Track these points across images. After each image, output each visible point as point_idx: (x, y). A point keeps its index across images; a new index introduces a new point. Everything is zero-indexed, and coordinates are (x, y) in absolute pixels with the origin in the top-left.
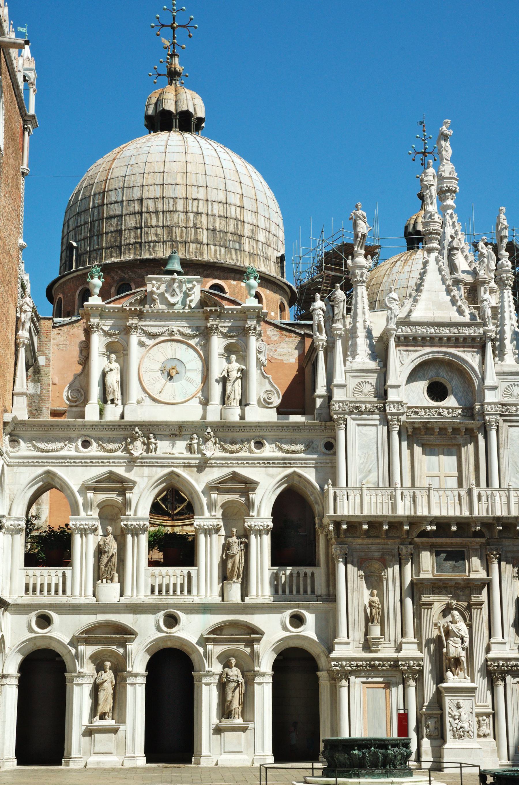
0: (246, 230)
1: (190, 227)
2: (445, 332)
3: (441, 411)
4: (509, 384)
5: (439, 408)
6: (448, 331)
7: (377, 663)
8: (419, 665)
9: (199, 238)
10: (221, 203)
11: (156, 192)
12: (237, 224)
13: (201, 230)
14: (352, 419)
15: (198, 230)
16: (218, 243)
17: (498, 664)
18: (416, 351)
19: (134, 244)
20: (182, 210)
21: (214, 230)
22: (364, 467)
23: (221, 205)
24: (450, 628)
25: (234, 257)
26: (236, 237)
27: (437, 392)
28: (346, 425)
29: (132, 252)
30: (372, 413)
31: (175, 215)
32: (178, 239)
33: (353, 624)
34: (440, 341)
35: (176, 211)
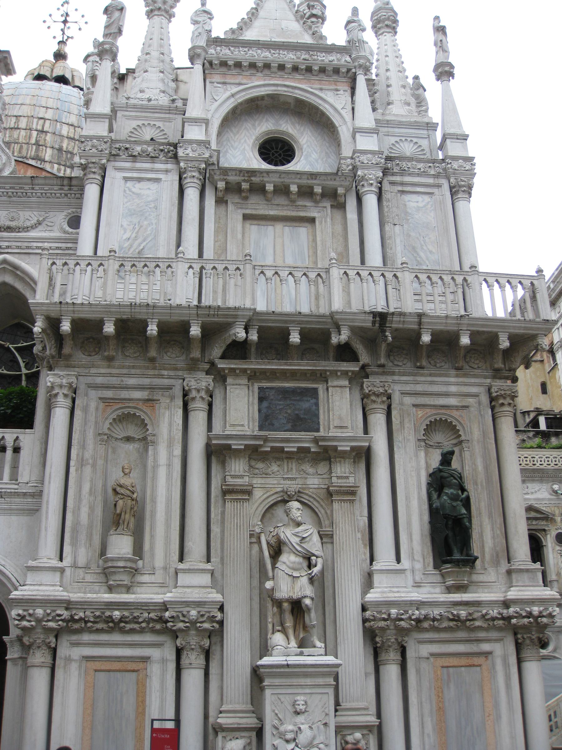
1: (31, 144)
2: (289, 57)
4: (398, 139)
7: (117, 614)
8: (212, 619)
9: (40, 154)
10: (72, 125)
13: (44, 148)
14: (116, 169)
15: (41, 147)
17: (389, 615)
18: (240, 84)
20: (24, 128)
21: (60, 150)
22: (131, 246)
24: (282, 536)
27: (277, 150)
28: (104, 177)
30: (153, 159)
31: (16, 133)
33: (75, 530)
35: (18, 128)
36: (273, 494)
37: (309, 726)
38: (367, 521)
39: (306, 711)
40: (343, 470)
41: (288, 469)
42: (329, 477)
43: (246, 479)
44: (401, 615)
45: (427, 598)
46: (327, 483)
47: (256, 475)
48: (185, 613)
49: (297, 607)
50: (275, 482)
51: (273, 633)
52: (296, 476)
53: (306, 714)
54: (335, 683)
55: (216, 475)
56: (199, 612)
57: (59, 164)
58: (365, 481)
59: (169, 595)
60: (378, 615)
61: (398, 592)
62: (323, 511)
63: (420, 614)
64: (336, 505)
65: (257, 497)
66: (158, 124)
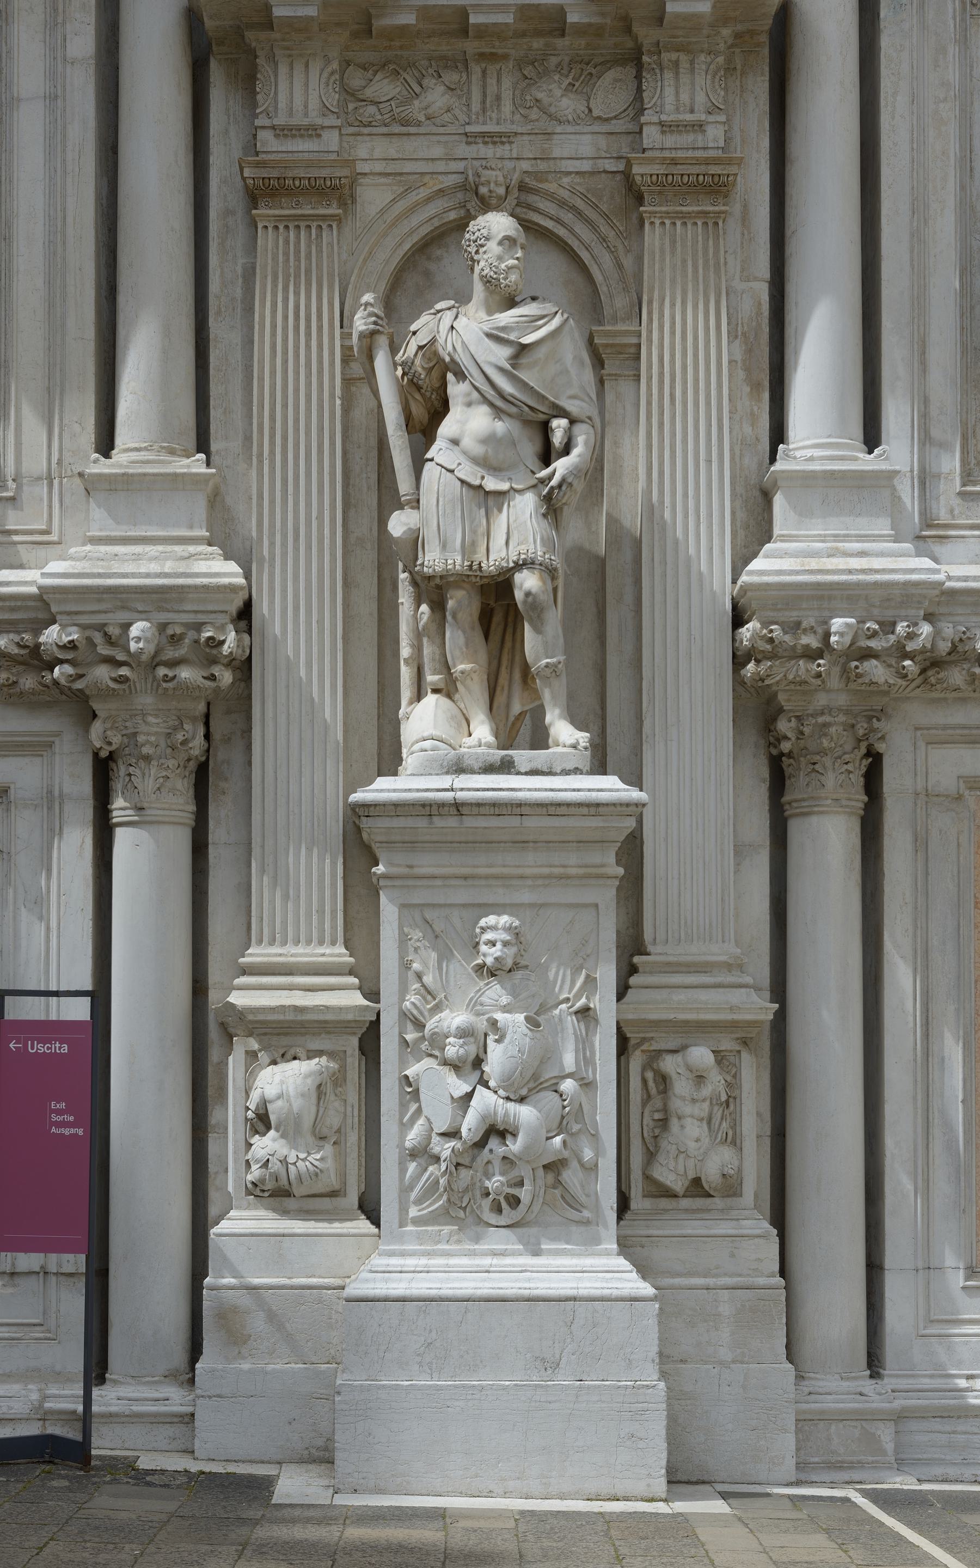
36: (429, 200)
37: (527, 1019)
38: (765, 298)
39: (515, 967)
40: (685, 97)
41: (484, 102)
42: (632, 127)
43: (331, 140)
44: (869, 638)
45: (966, 579)
46: (625, 151)
47: (369, 125)
48: (114, 631)
49: (497, 608)
50: (438, 151)
51: (419, 696)
52: (514, 128)
53: (519, 975)
54: (621, 871)
55: (227, 132)
56: (162, 627)
58: (766, 143)
59: (55, 566)
60: (787, 638)
61: (862, 554)
62: (607, 259)
63: (937, 633)
64: (653, 237)
65: (372, 210)
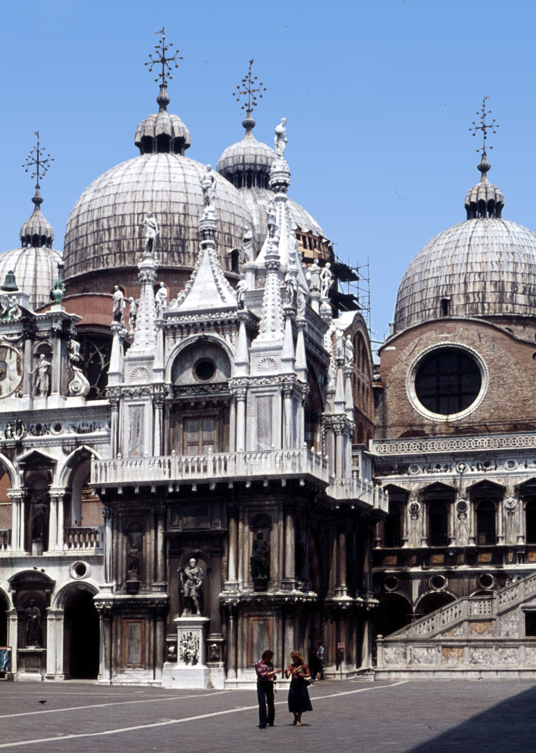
0: (191, 234)
2: (205, 318)
3: (205, 387)
5: (203, 385)
6: (207, 317)
11: (108, 212)
12: (180, 230)
16: (160, 249)
19: (93, 258)
23: (164, 215)
25: (176, 259)
26: (179, 242)
29: (91, 265)
30: (140, 394)
31: (123, 230)
32: (125, 250)
34: (202, 326)
35: (124, 226)
57: (158, 251)
66: (145, 367)
